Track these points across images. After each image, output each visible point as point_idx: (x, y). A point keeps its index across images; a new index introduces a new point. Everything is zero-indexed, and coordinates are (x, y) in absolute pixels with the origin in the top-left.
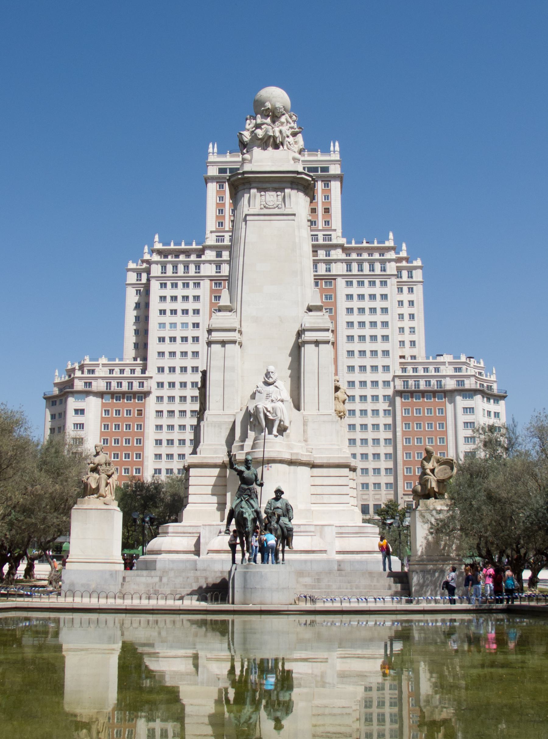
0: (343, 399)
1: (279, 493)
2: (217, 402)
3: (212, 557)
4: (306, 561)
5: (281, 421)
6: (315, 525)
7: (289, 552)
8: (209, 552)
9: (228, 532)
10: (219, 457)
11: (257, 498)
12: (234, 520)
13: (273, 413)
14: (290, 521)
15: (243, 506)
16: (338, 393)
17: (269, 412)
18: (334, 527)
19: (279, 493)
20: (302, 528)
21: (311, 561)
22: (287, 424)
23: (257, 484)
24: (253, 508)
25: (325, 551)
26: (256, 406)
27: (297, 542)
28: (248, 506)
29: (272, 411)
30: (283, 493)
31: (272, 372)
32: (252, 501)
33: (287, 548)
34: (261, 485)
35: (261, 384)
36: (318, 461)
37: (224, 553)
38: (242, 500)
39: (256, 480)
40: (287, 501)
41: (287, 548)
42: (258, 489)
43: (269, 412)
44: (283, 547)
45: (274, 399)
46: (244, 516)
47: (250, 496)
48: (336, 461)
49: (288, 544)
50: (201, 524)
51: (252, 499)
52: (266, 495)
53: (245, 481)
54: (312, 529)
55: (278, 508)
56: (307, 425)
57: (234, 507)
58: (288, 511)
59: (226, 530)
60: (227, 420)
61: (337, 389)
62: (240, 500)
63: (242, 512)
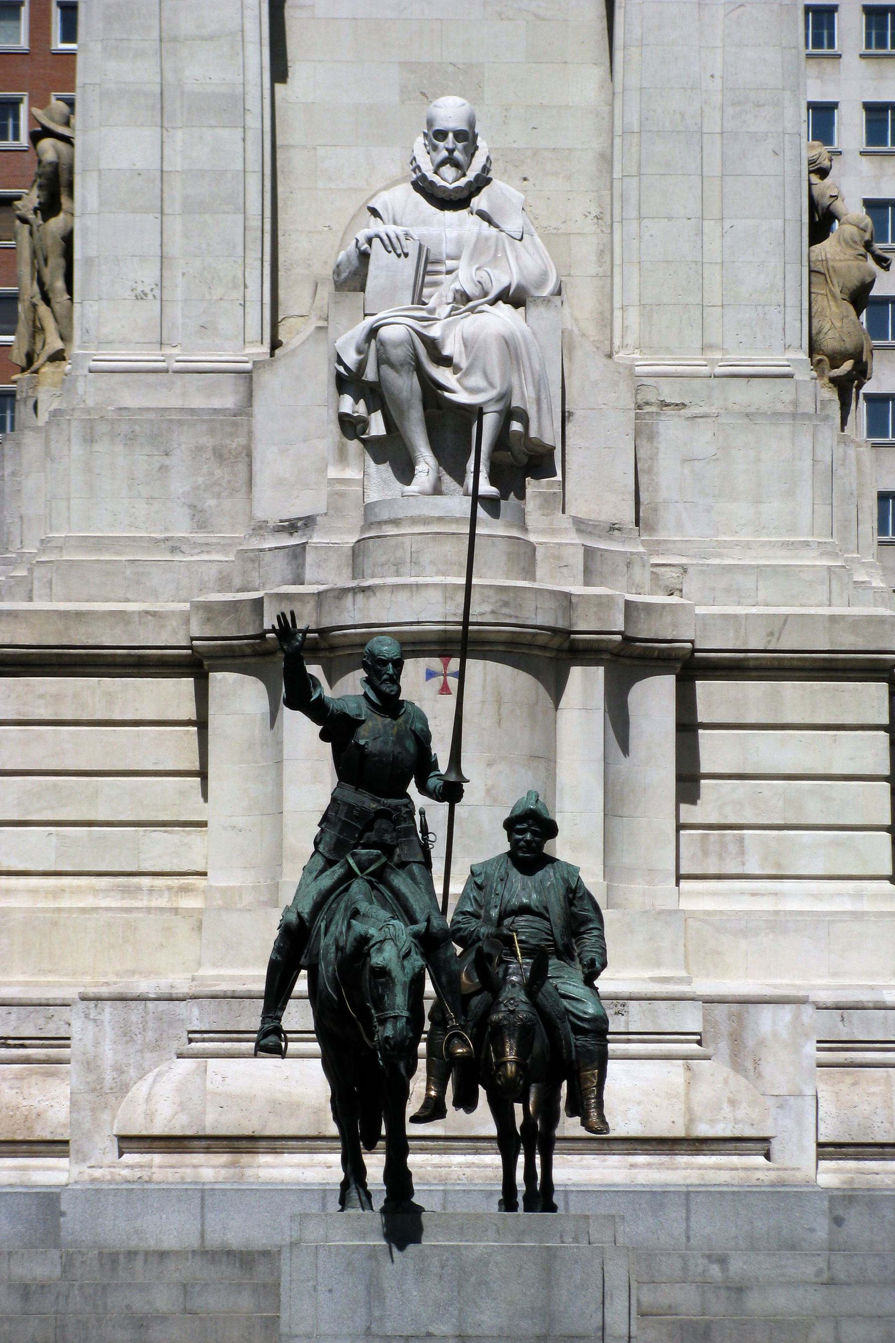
0: (853, 282)
1: (531, 831)
2: (141, 297)
3: (145, 1174)
4: (656, 1198)
5: (509, 414)
6: (709, 1001)
7: (576, 1145)
8: (129, 1142)
9: (272, 1040)
10: (154, 614)
11: (427, 864)
12: (302, 985)
13: (468, 372)
14: (589, 979)
15: (363, 906)
16: (828, 247)
17: (447, 362)
18: (808, 1011)
19: (531, 831)
20: (636, 1018)
21: (687, 1196)
22: (545, 430)
23: (423, 789)
24: (413, 921)
25: (762, 1144)
26: (373, 332)
27: (633, 1091)
28: (384, 904)
29: (460, 359)
30: (550, 829)
31: (460, 135)
32: (400, 881)
33: (570, 1126)
34: (452, 792)
35: (403, 200)
36: (716, 641)
37: (207, 1150)
38: (349, 875)
39: (422, 764)
40: (573, 871)
41: (570, 1126)
42: (433, 812)
43: (447, 362)
44: (552, 1120)
45: (470, 289)
46: (377, 960)
47: (388, 850)
48: (819, 641)
49: (576, 1107)
50: (71, 993)
51: (403, 865)
52: (466, 843)
53: (351, 764)
54: (691, 1019)
55: (525, 910)
56: (651, 438)
57: (306, 909)
58: (575, 928)
59: (264, 1034)
60: (198, 402)
61: (821, 221)
62: (338, 871)
63: (364, 940)
